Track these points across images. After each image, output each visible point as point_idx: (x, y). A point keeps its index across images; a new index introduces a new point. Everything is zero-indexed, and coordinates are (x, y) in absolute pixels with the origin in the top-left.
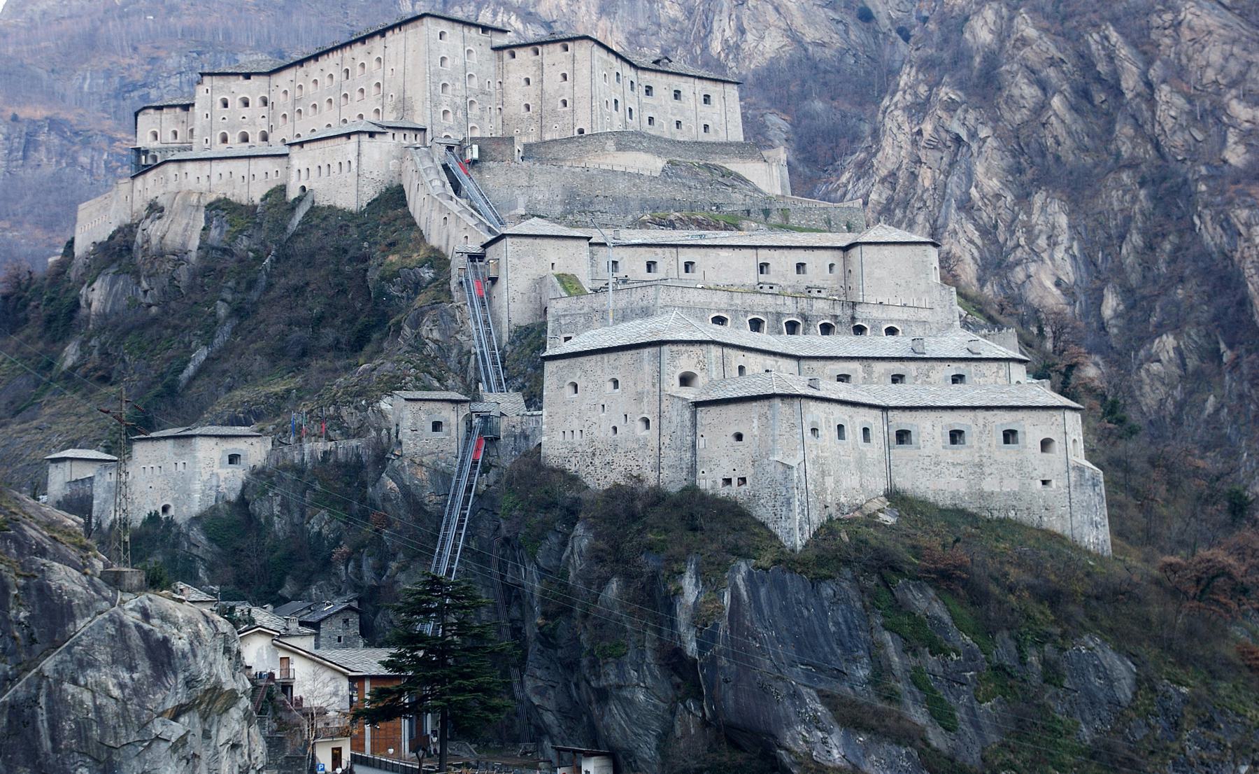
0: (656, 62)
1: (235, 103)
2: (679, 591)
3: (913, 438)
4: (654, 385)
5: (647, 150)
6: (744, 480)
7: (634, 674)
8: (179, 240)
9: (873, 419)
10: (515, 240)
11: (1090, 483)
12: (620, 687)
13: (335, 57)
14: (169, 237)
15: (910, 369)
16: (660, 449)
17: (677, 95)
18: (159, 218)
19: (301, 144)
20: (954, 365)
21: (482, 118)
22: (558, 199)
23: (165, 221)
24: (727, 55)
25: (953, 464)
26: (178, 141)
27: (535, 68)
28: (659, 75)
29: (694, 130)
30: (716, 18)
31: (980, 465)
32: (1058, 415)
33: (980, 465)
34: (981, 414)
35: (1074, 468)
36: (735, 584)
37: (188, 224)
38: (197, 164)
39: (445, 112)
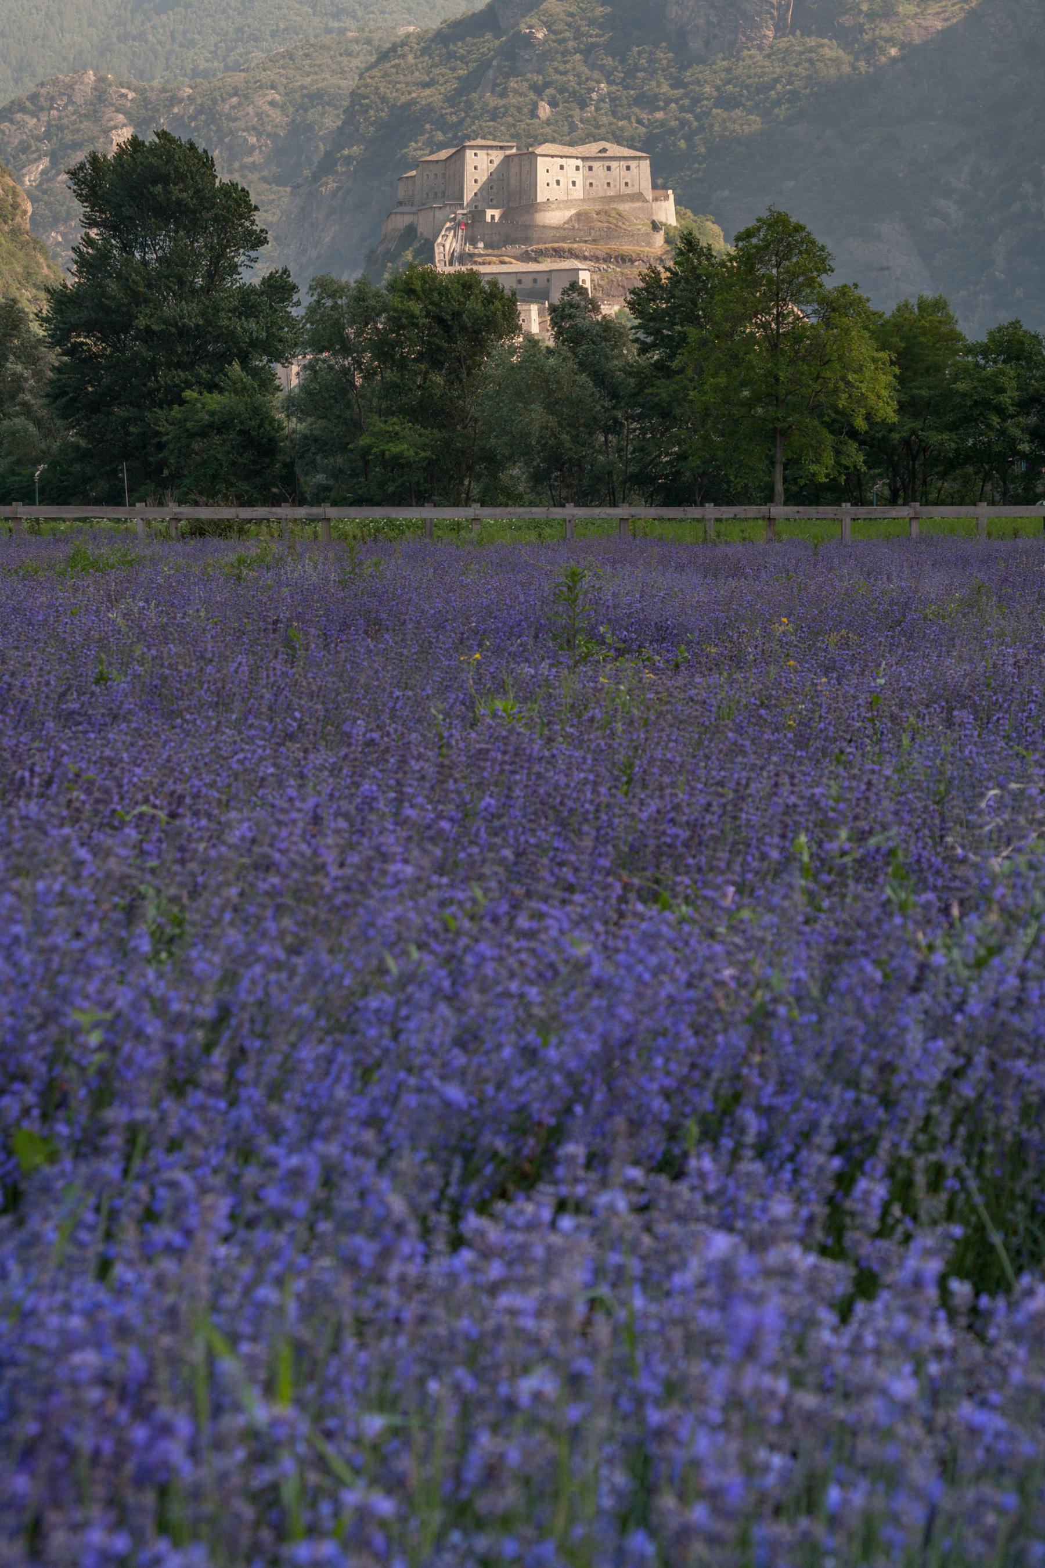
17: (609, 168)
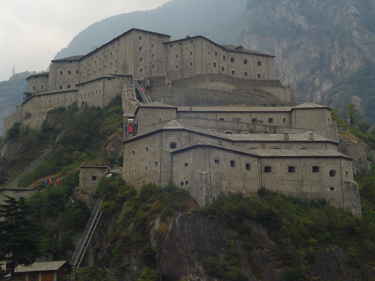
0: (236, 49)
1: (65, 73)
2: (153, 225)
3: (272, 170)
4: (159, 148)
5: (225, 82)
6: (187, 182)
7: (134, 260)
8: (34, 126)
9: (254, 163)
10: (144, 109)
11: (352, 189)
12: (128, 265)
13: (102, 51)
14: (31, 125)
15: (283, 145)
16: (161, 173)
17: (245, 62)
18: (29, 118)
19: (83, 84)
20: (302, 144)
21: (158, 72)
22: (183, 101)
23: (31, 119)
24: (337, 72)
25: (290, 180)
26: (43, 89)
27: (180, 51)
28: (237, 54)
29: (253, 76)
30: (333, 56)
31: (302, 181)
32: (338, 161)
33: (302, 181)
34: (302, 161)
35: (345, 183)
36: (175, 221)
37: (39, 120)
38: (46, 97)
39: (141, 70)
